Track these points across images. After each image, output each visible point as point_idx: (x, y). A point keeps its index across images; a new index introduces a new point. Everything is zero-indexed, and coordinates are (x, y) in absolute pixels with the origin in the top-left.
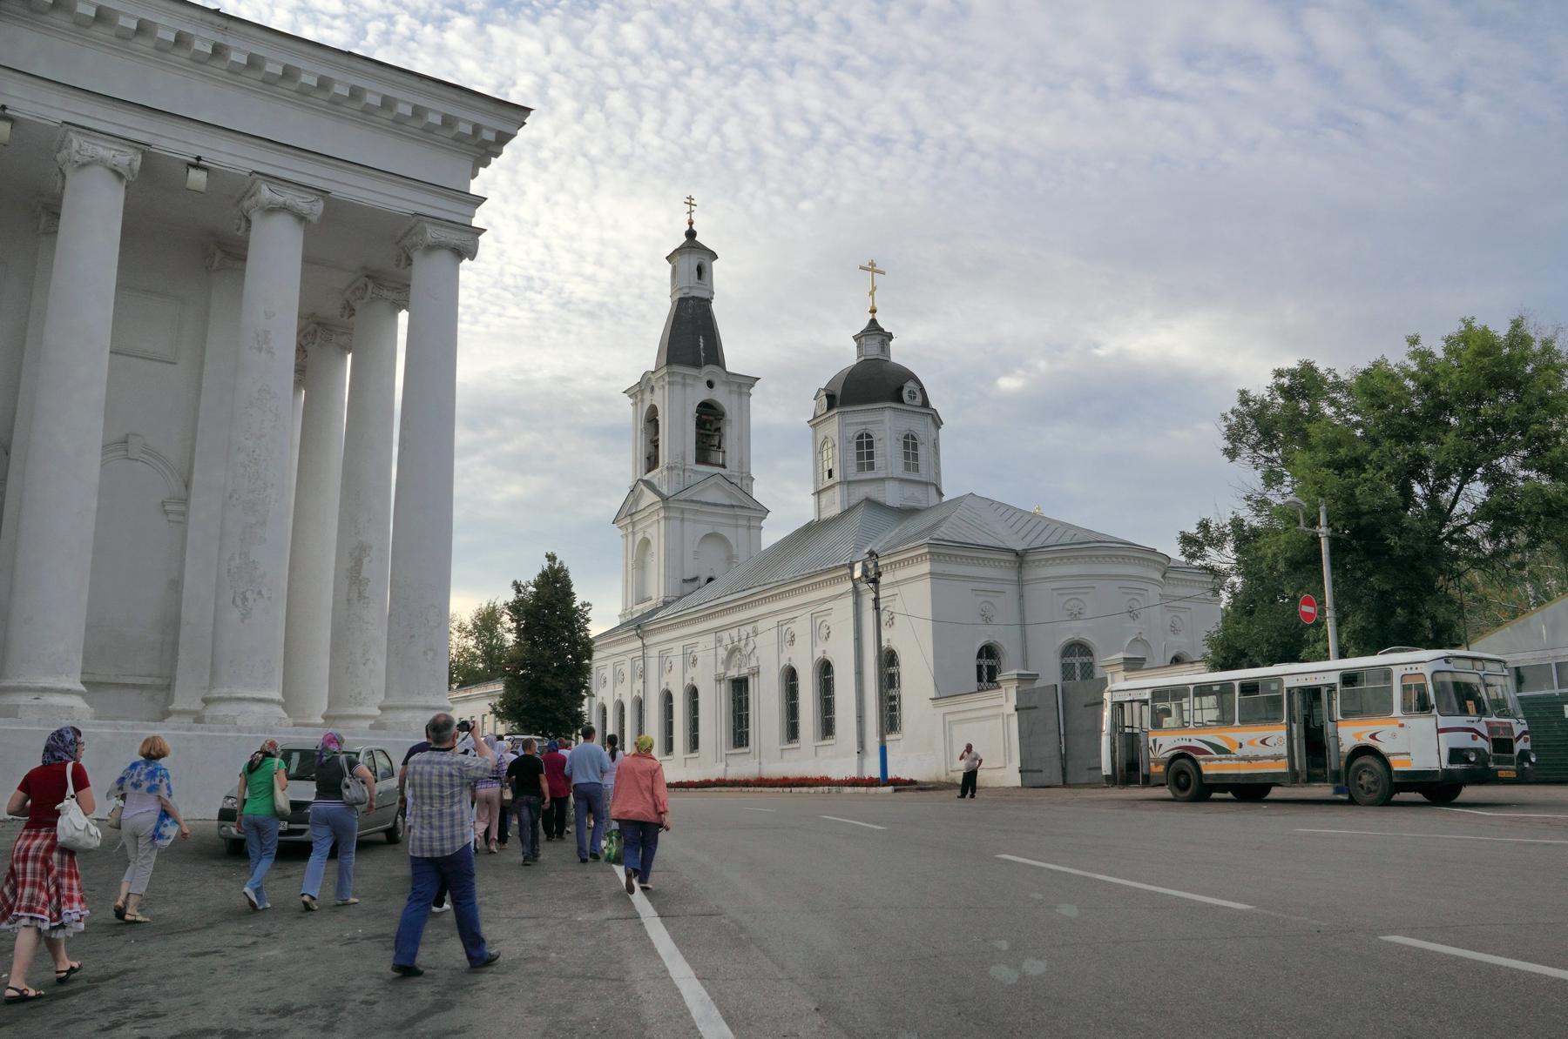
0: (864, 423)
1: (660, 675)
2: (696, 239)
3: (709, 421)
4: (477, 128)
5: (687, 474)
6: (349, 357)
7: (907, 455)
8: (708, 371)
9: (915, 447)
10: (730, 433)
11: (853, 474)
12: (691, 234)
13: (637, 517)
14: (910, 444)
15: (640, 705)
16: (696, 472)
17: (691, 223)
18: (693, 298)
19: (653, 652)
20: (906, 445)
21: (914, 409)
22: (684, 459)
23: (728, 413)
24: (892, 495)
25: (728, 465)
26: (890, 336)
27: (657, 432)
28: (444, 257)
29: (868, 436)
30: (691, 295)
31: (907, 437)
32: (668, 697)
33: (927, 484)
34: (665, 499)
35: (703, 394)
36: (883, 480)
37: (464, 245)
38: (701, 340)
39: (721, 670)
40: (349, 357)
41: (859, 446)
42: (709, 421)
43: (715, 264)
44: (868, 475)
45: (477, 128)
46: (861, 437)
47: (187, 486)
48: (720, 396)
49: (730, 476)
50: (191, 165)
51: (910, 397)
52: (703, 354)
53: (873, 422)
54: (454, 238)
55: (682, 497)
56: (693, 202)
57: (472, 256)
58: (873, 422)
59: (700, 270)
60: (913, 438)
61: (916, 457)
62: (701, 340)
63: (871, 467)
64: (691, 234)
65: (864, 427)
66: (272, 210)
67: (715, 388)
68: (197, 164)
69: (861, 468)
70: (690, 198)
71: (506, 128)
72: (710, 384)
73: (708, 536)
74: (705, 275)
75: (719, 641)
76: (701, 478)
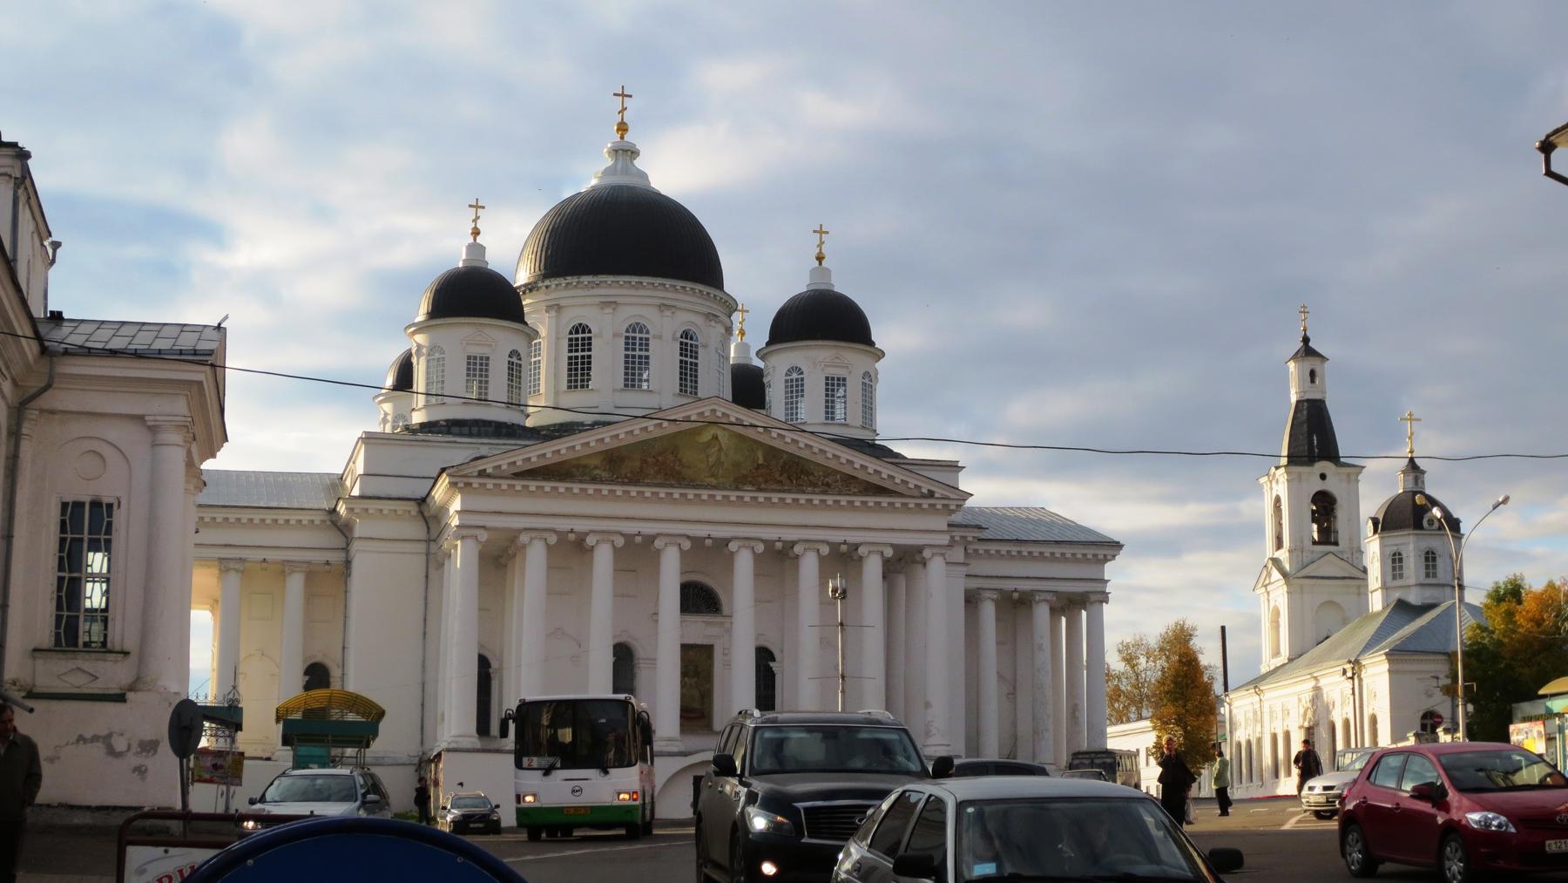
0: (1396, 545)
1: (1271, 722)
2: (1310, 344)
3: (1324, 507)
4: (1105, 556)
5: (1304, 554)
6: (1064, 619)
7: (1427, 567)
8: (1323, 466)
9: (1434, 559)
10: (1341, 513)
11: (1390, 583)
12: (1306, 340)
13: (1269, 588)
14: (1430, 558)
15: (1259, 740)
16: (1313, 552)
17: (1305, 330)
18: (1308, 401)
19: (1266, 705)
20: (1427, 559)
21: (1432, 532)
22: (1302, 542)
23: (1338, 499)
24: (1414, 598)
25: (1340, 542)
26: (1423, 472)
27: (1281, 518)
28: (1097, 605)
29: (1400, 554)
30: (1306, 398)
31: (1427, 553)
32: (1274, 738)
33: (1444, 585)
34: (1285, 575)
35: (1319, 486)
36: (1409, 586)
37: (1104, 597)
38: (1315, 438)
39: (1301, 724)
40: (1064, 619)
41: (1394, 561)
42: (1324, 507)
43: (1327, 364)
44: (1399, 582)
45: (1105, 556)
46: (1394, 555)
47: (1015, 688)
48: (1331, 485)
49: (1341, 552)
50: (1013, 591)
51: (1429, 524)
52: (1316, 450)
53: (1402, 544)
54: (1099, 597)
55: (1299, 575)
56: (1306, 310)
57: (1107, 603)
58: (1402, 544)
59: (1313, 374)
60: (1433, 553)
61: (1434, 567)
62: (1315, 438)
63: (1401, 576)
64: (1306, 340)
65: (1395, 548)
66: (1040, 601)
67: (1327, 479)
68: (1016, 590)
69: (1394, 577)
70: (1304, 307)
71: (1114, 553)
72: (1323, 477)
73: (1322, 604)
74: (1317, 381)
75: (1300, 700)
76: (1316, 556)
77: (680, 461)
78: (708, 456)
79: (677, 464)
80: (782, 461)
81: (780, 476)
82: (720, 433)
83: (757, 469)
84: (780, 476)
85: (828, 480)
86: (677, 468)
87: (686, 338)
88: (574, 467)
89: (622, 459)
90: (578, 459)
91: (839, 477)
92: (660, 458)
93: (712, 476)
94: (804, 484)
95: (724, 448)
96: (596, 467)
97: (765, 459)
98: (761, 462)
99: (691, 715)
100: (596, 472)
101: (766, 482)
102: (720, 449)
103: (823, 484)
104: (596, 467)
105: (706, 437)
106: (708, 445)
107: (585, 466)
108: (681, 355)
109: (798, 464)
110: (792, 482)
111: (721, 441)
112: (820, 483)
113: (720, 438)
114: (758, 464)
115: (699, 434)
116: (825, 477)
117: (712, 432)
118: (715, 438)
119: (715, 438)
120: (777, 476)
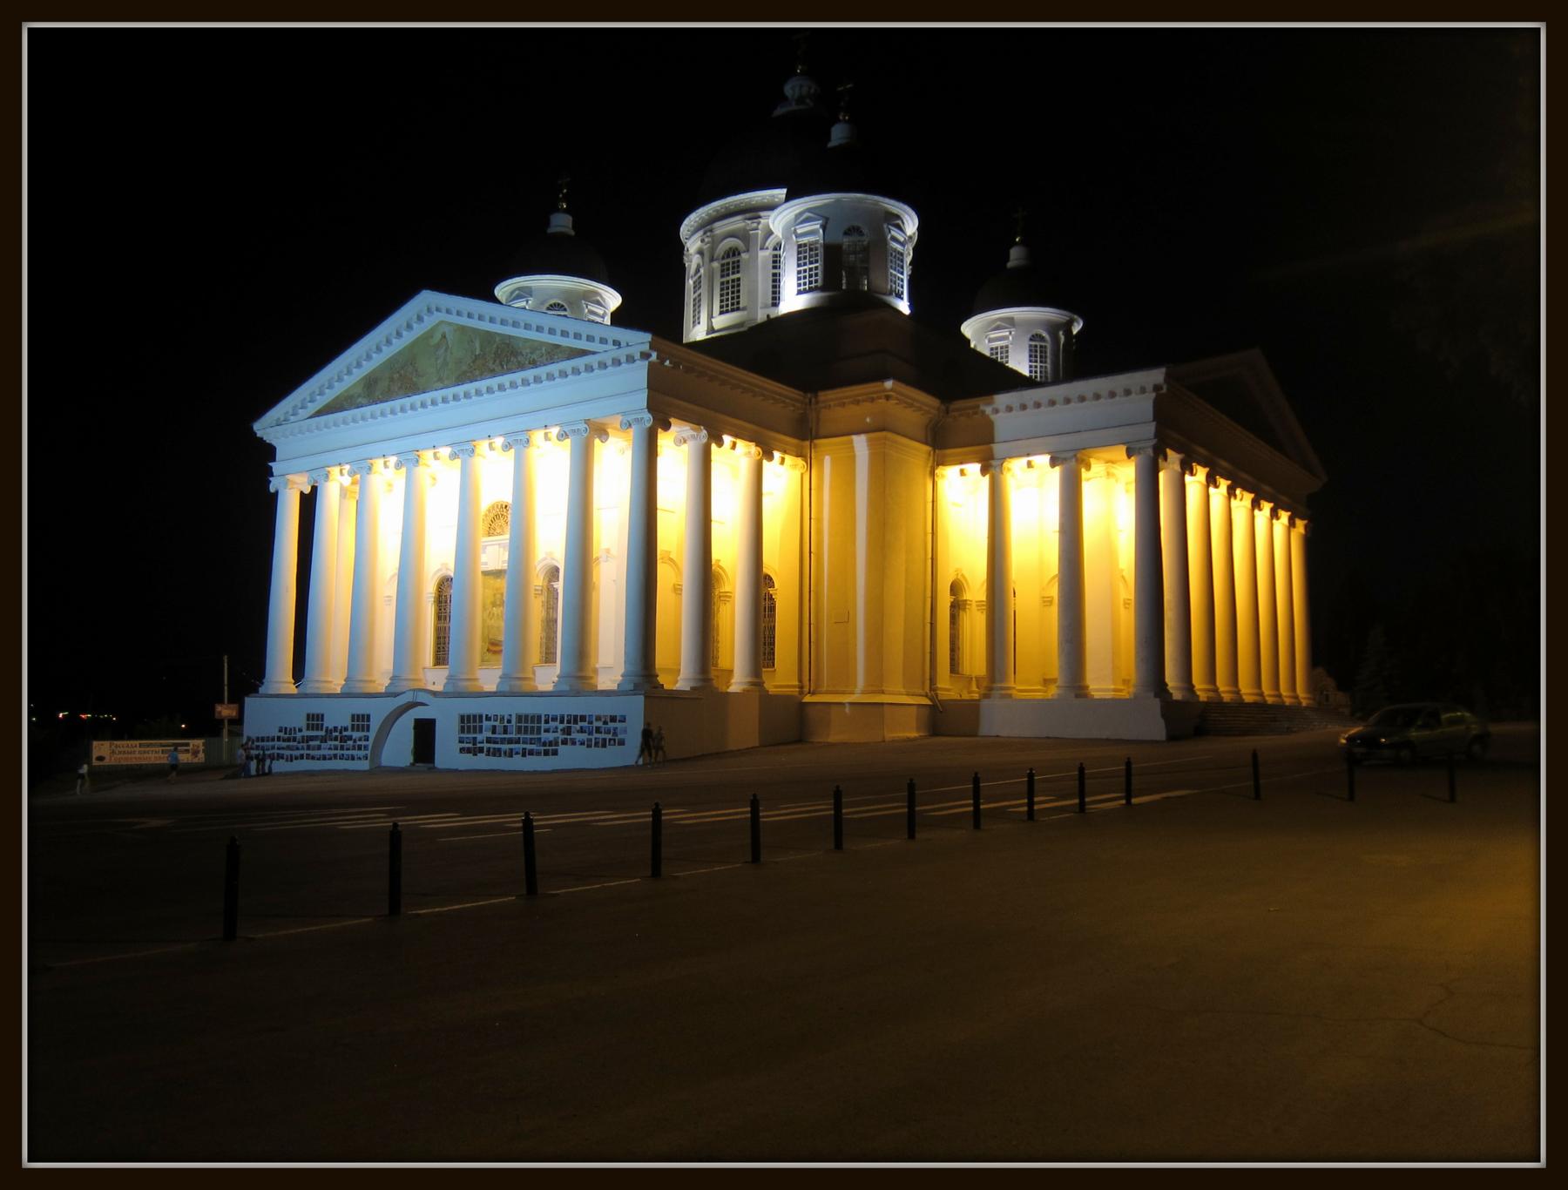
77: (416, 371)
78: (437, 359)
79: (414, 373)
80: (495, 346)
82: (447, 329)
83: (474, 362)
84: (494, 364)
85: (534, 356)
86: (414, 379)
90: (346, 391)
92: (402, 372)
94: (514, 367)
97: (481, 350)
98: (477, 353)
100: (360, 400)
103: (530, 363)
104: (359, 396)
105: (438, 336)
106: (438, 346)
109: (508, 345)
110: (503, 367)
111: (448, 339)
112: (527, 362)
114: (476, 356)
115: (432, 337)
116: (531, 353)
118: (444, 336)
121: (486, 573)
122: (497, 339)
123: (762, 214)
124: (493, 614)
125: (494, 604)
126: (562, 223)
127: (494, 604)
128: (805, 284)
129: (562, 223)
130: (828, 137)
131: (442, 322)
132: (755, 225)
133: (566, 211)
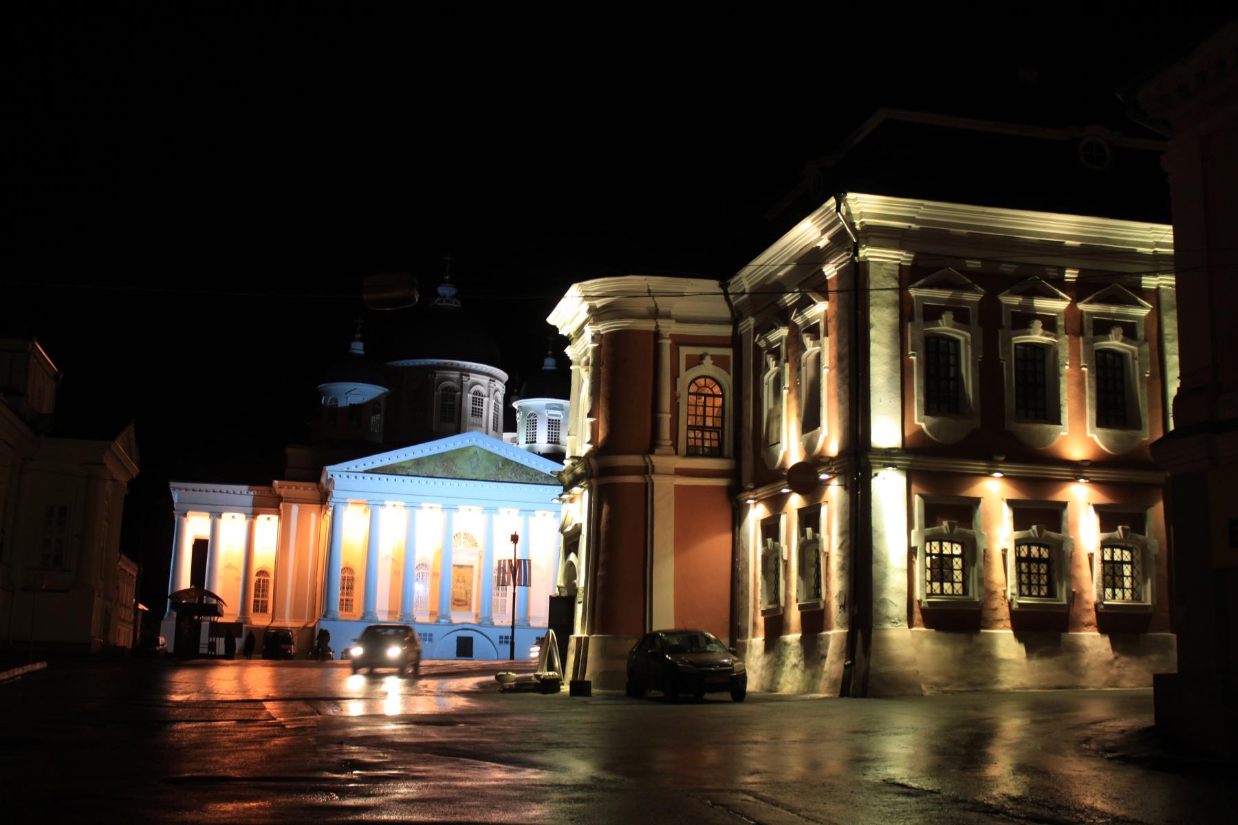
77: (456, 465)
78: (471, 463)
81: (511, 474)
84: (511, 474)
86: (454, 469)
87: (477, 395)
88: (398, 467)
89: (424, 464)
90: (400, 463)
91: (543, 476)
93: (474, 473)
95: (480, 458)
96: (410, 468)
99: (461, 603)
101: (503, 477)
102: (478, 460)
104: (410, 468)
105: (471, 452)
106: (471, 457)
107: (404, 467)
108: (473, 404)
113: (478, 453)
116: (535, 476)
117: (474, 450)
118: (476, 453)
119: (476, 453)
120: (510, 476)
121: (454, 566)
122: (514, 464)
123: (470, 374)
124: (457, 586)
125: (458, 581)
126: (358, 347)
127: (458, 581)
128: (552, 439)
129: (358, 347)
130: (542, 364)
131: (474, 446)
132: (466, 379)
133: (360, 340)
